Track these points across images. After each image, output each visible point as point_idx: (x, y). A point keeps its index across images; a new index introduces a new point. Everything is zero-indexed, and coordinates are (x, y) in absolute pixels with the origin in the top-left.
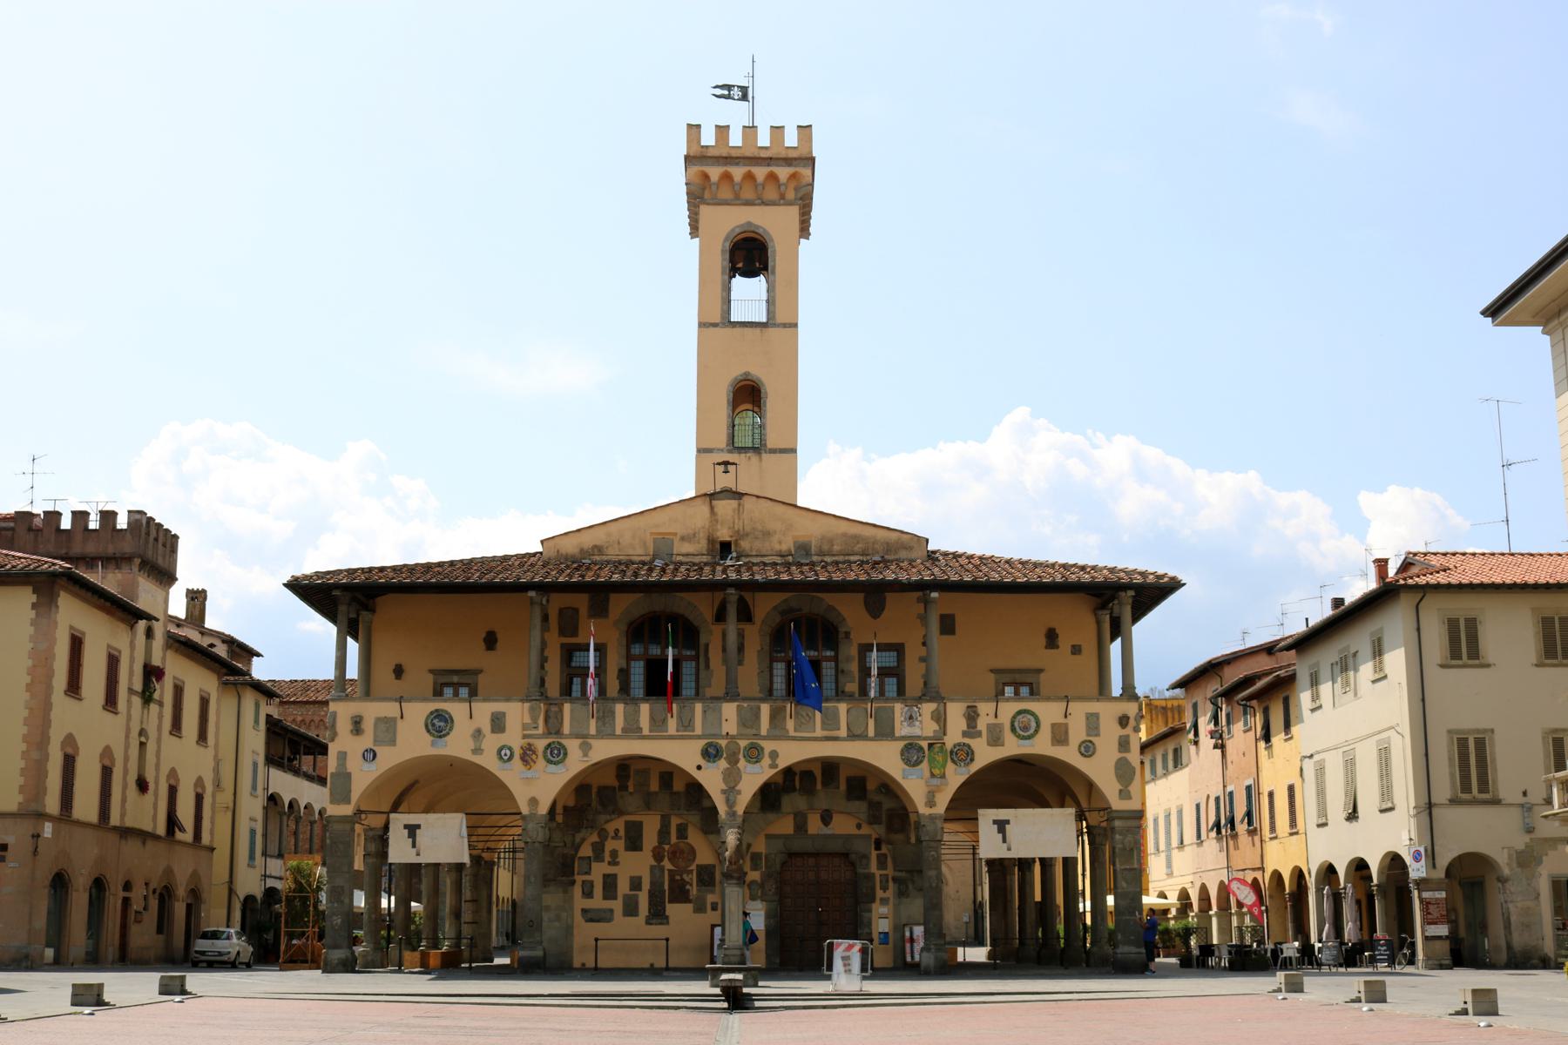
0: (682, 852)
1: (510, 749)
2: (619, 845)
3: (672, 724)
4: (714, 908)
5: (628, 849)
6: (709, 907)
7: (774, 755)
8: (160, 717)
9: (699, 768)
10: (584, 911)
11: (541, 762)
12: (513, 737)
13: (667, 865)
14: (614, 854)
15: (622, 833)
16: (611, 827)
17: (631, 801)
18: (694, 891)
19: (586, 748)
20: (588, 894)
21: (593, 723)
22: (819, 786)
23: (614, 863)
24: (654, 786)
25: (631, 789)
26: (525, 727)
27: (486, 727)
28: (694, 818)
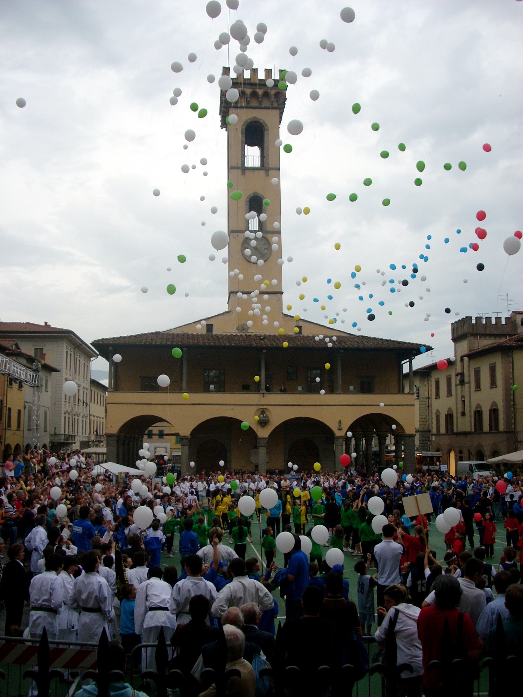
8: (470, 387)
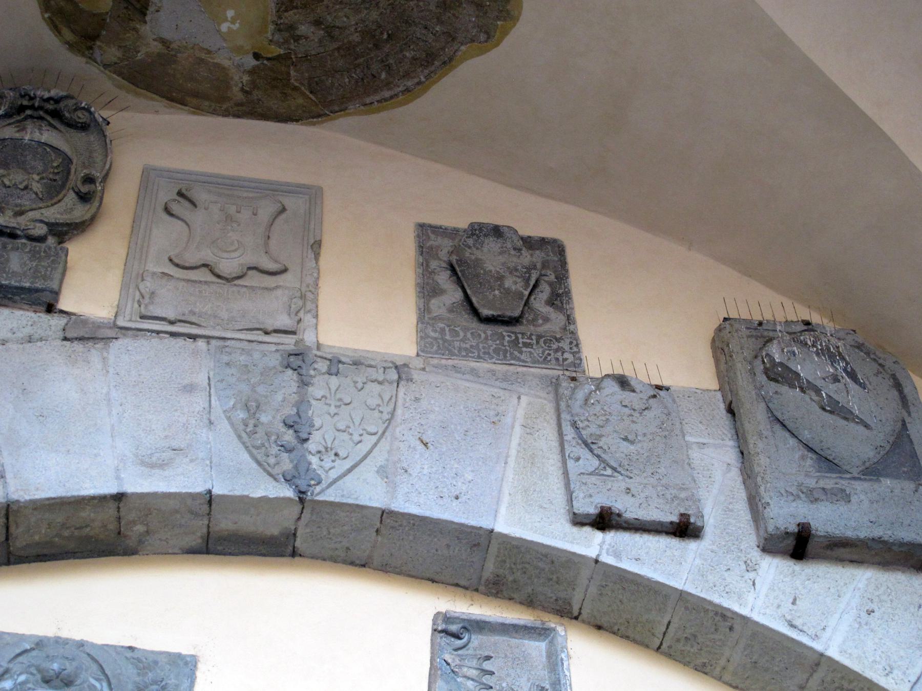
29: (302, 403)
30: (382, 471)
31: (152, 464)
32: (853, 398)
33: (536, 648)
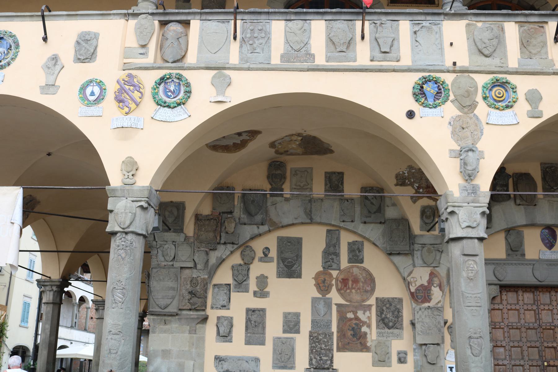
0: (356, 281)
1: (100, 84)
2: (270, 269)
3: (363, 53)
4: (402, 360)
5: (280, 275)
6: (394, 358)
7: (534, 98)
9: (411, 115)
10: (219, 359)
11: (148, 104)
12: (108, 69)
13: (335, 297)
14: (262, 281)
15: (273, 253)
16: (258, 246)
17: (286, 209)
18: (373, 334)
19: (221, 84)
20: (225, 336)
21: (235, 47)
22: (540, 193)
23: (261, 293)
24: (318, 189)
25: (287, 192)
26: (127, 52)
27: (67, 53)
28: (374, 232)
29: (311, 208)
30: (320, 217)
31: (296, 219)
32: (374, 201)
33: (337, 232)
